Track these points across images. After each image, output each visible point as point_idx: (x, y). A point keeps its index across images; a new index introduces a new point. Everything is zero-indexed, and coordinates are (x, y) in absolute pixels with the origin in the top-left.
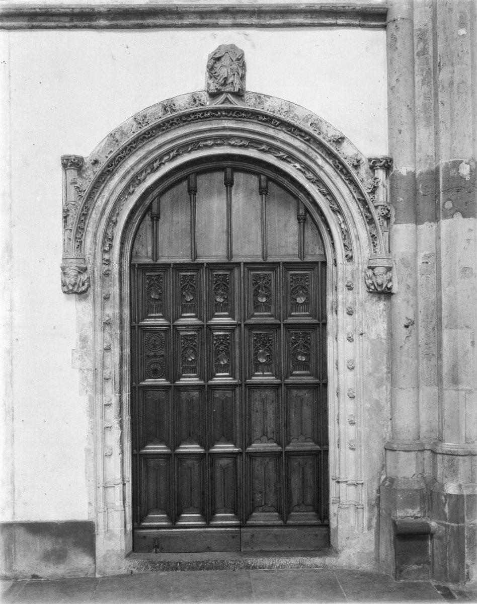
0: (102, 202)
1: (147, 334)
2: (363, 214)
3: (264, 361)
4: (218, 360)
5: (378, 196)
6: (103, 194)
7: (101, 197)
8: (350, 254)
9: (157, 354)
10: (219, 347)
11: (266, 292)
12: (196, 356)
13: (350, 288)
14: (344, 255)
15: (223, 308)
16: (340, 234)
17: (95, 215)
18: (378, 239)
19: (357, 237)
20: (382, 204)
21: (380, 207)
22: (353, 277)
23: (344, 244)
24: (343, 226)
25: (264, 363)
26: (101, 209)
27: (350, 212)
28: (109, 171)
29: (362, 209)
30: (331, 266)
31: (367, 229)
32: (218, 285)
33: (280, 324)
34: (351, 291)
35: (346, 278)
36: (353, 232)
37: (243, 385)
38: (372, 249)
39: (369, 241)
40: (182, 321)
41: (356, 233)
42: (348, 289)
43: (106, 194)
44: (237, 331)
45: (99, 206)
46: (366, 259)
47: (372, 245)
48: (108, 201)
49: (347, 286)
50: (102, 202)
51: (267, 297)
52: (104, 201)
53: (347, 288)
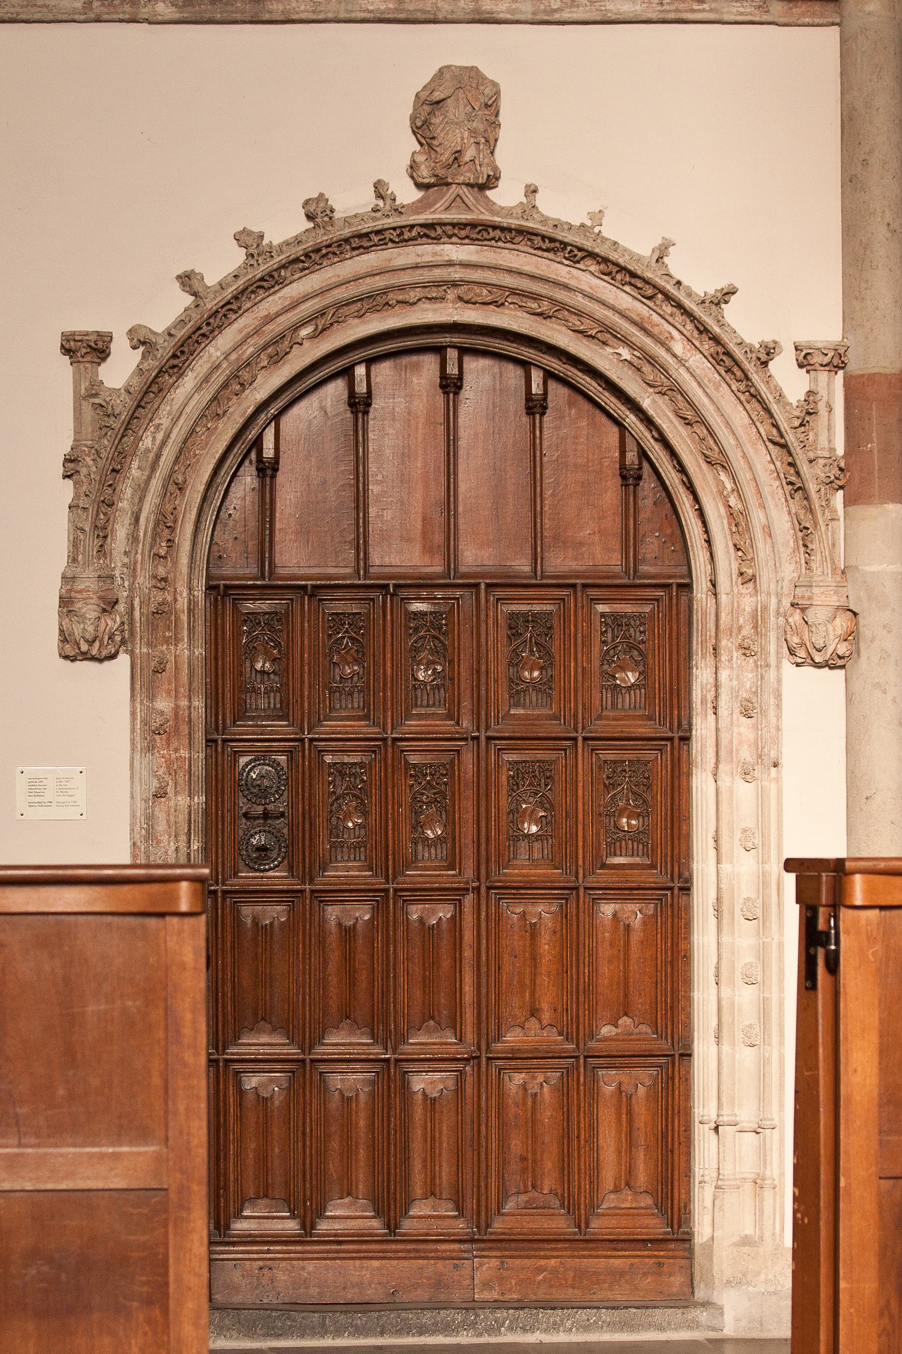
0: (154, 438)
1: (243, 760)
2: (782, 476)
3: (534, 829)
4: (418, 826)
5: (816, 435)
6: (157, 421)
7: (152, 429)
8: (750, 572)
9: (271, 807)
10: (423, 794)
11: (540, 658)
12: (365, 814)
13: (746, 650)
14: (735, 572)
15: (431, 696)
16: (725, 521)
17: (135, 471)
18: (816, 536)
19: (768, 531)
20: (827, 454)
21: (821, 462)
22: (755, 627)
23: (735, 545)
24: (733, 501)
25: (532, 835)
26: (151, 456)
27: (751, 468)
28: (174, 366)
29: (778, 464)
30: (704, 596)
31: (789, 513)
32: (421, 637)
33: (575, 739)
34: (751, 660)
35: (740, 628)
36: (757, 518)
37: (483, 890)
38: (803, 561)
39: (796, 541)
40: (329, 727)
41: (763, 520)
42: (744, 654)
43: (164, 420)
44: (468, 758)
45: (148, 451)
46: (786, 584)
47: (802, 549)
48: (169, 436)
49: (741, 647)
50: (154, 438)
51: (541, 669)
52: (160, 436)
53: (740, 652)
